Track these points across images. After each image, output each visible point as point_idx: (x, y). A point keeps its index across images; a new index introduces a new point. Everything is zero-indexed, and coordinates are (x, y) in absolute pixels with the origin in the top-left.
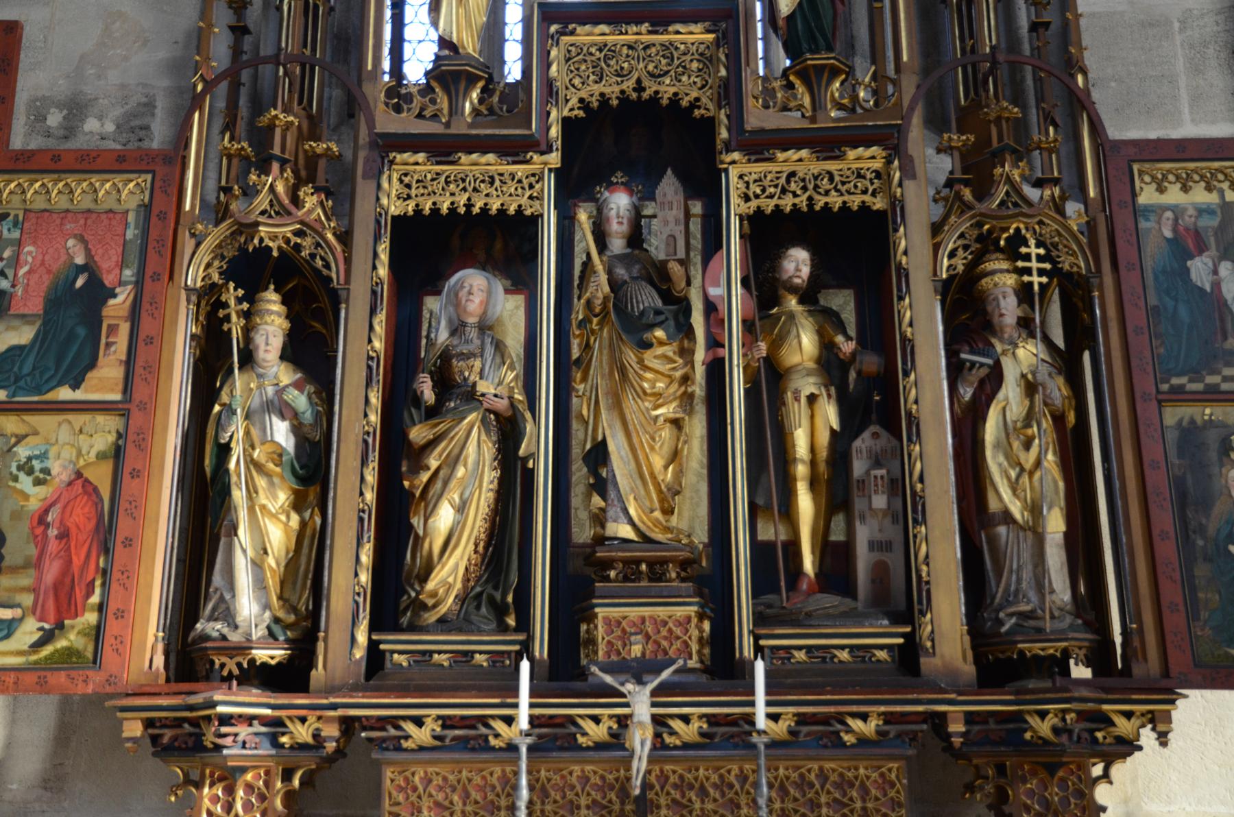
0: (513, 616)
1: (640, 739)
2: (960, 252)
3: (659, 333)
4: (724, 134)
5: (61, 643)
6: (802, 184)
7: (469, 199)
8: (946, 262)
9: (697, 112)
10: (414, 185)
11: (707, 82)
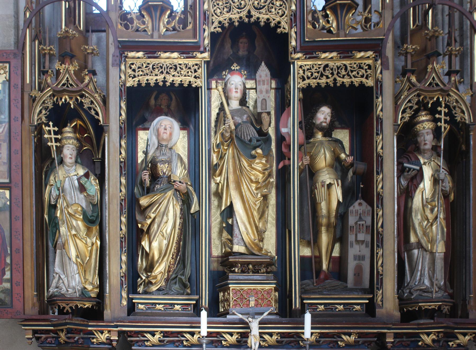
2: (408, 110)
3: (259, 151)
6: (331, 72)
7: (165, 78)
8: (400, 117)
9: (279, 30)
10: (137, 71)
11: (284, 12)
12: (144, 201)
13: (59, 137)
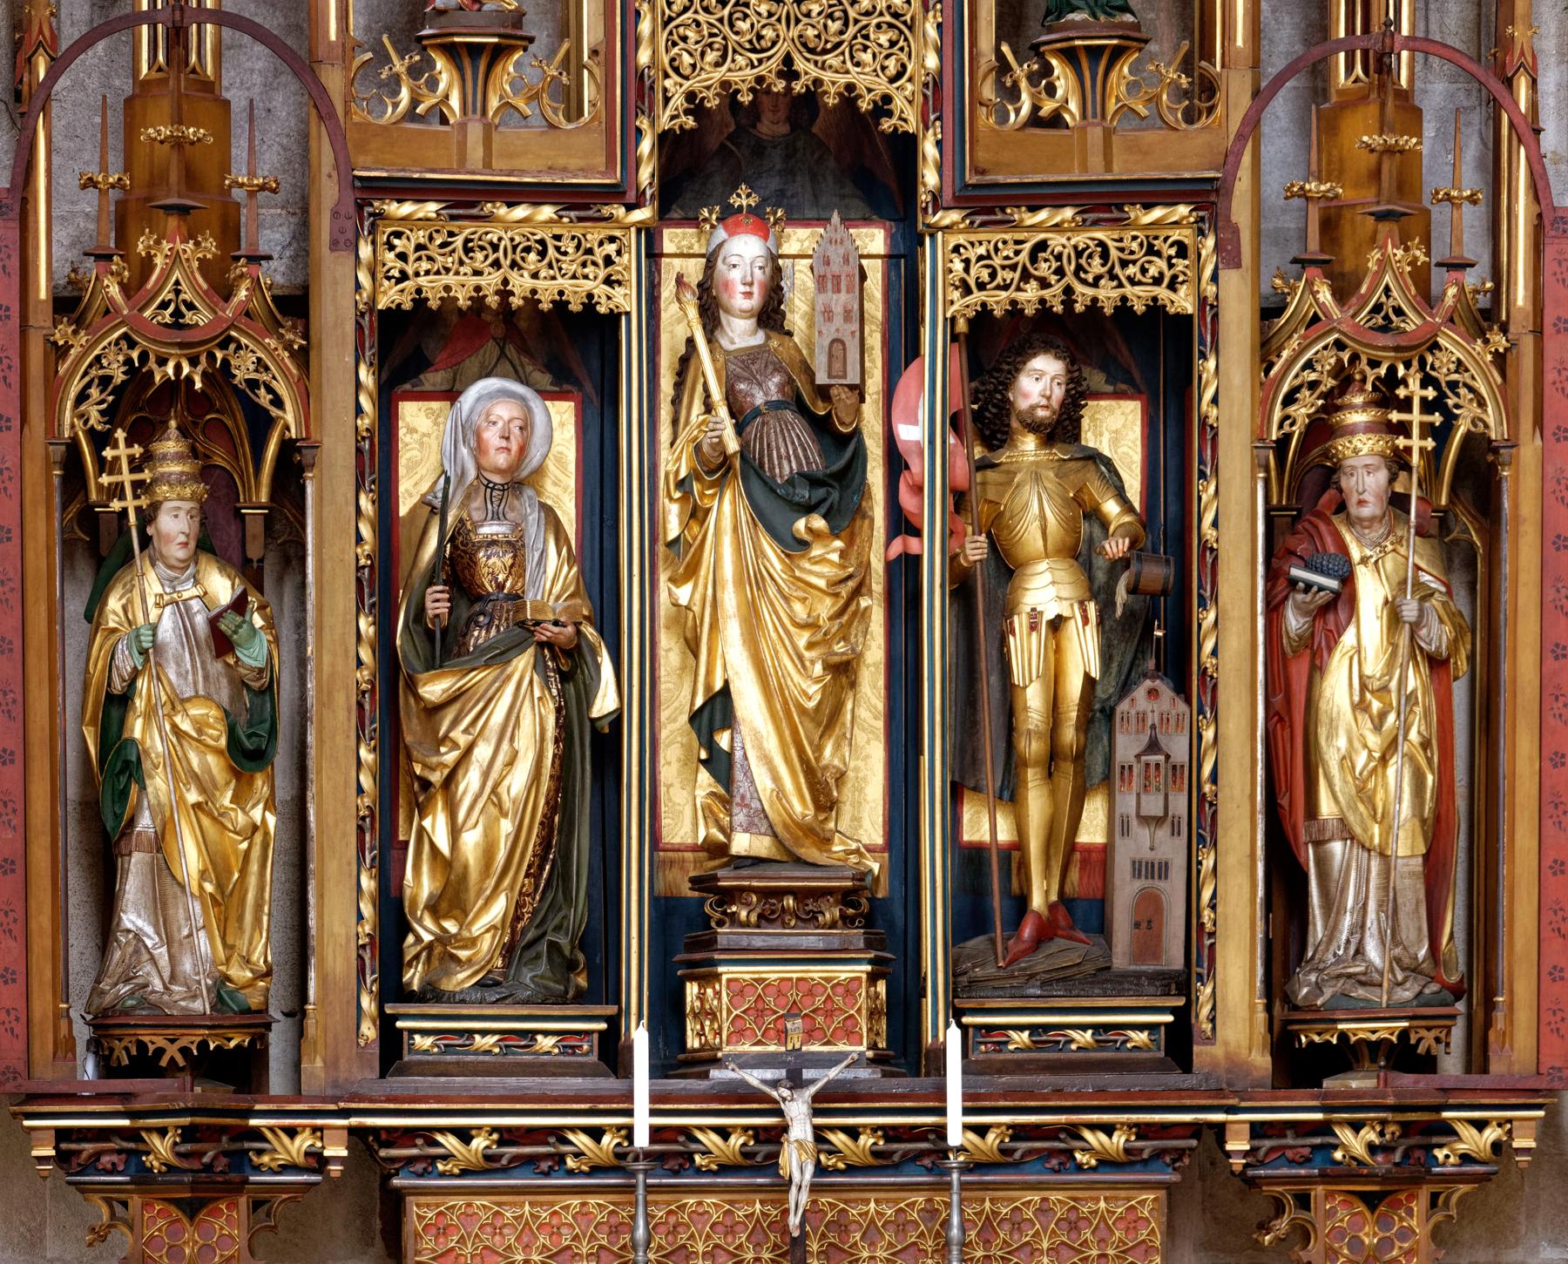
0: (584, 975)
1: (796, 1161)
4: (930, 178)
6: (1055, 265)
7: (506, 282)
8: (1277, 414)
9: (886, 125)
10: (412, 258)
11: (904, 67)
12: (434, 689)
13: (146, 475)
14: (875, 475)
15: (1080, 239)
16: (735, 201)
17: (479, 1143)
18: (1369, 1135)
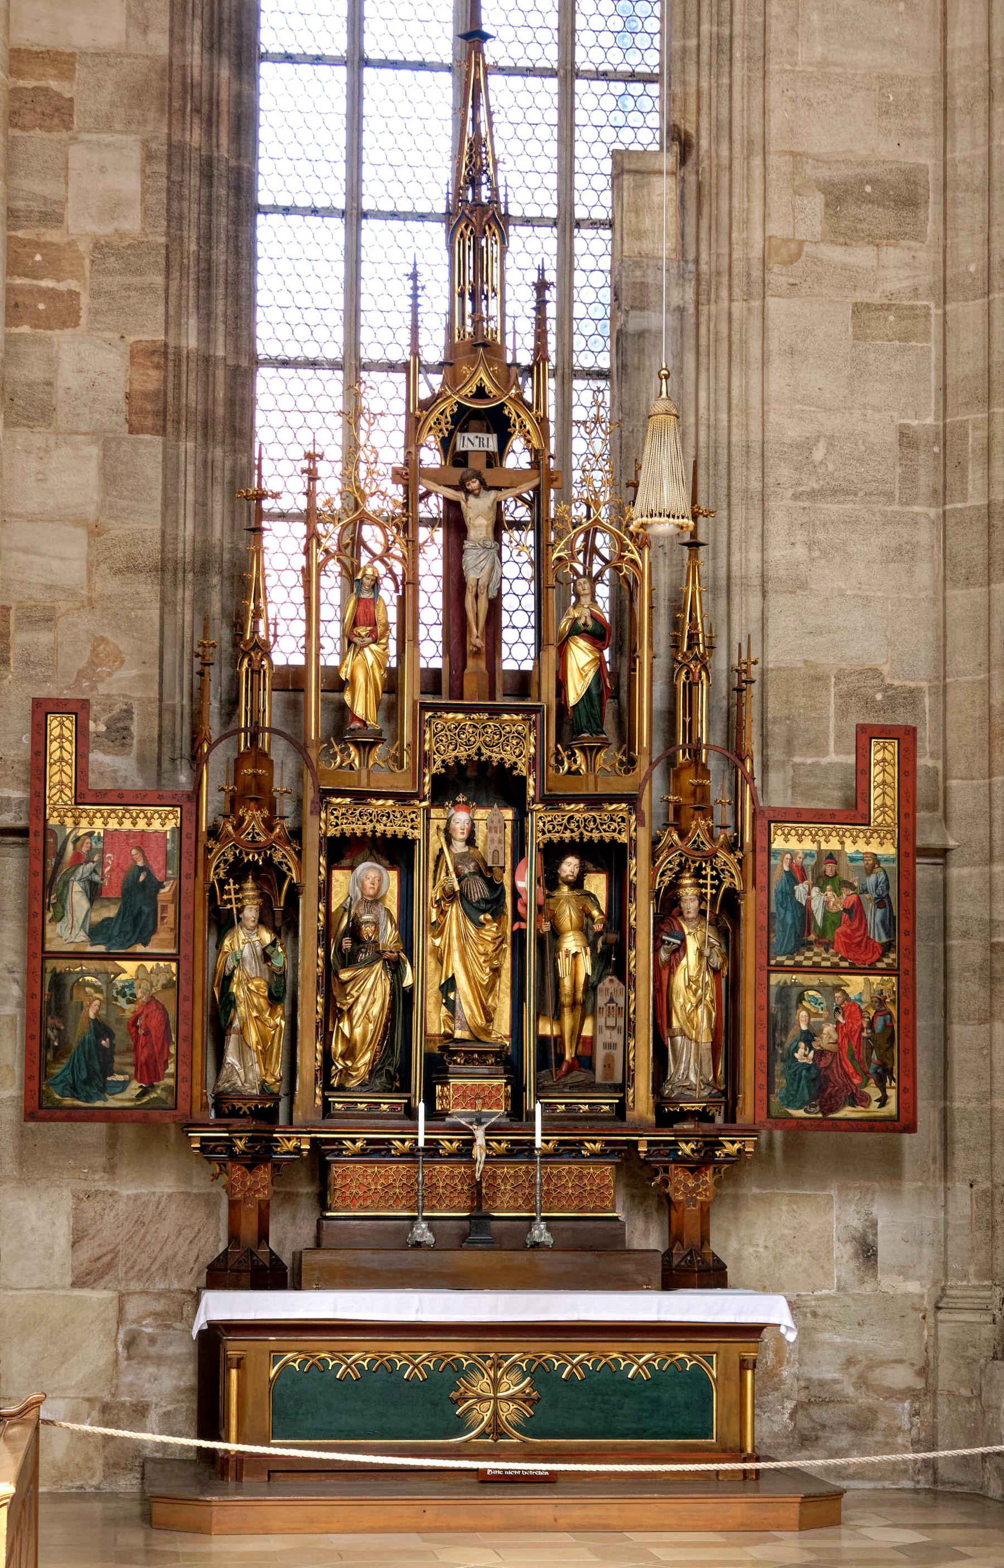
1: (479, 1152)
4: (531, 792)
5: (154, 1095)
9: (515, 773)
12: (345, 976)
13: (240, 896)
14: (508, 900)
15: (586, 815)
16: (458, 799)
17: (359, 1144)
18: (692, 1146)
